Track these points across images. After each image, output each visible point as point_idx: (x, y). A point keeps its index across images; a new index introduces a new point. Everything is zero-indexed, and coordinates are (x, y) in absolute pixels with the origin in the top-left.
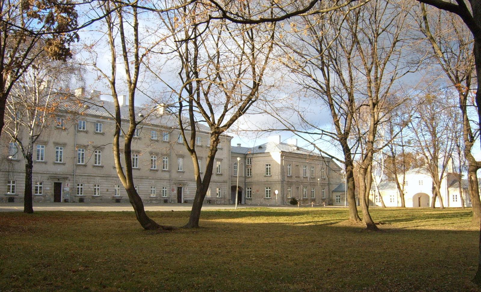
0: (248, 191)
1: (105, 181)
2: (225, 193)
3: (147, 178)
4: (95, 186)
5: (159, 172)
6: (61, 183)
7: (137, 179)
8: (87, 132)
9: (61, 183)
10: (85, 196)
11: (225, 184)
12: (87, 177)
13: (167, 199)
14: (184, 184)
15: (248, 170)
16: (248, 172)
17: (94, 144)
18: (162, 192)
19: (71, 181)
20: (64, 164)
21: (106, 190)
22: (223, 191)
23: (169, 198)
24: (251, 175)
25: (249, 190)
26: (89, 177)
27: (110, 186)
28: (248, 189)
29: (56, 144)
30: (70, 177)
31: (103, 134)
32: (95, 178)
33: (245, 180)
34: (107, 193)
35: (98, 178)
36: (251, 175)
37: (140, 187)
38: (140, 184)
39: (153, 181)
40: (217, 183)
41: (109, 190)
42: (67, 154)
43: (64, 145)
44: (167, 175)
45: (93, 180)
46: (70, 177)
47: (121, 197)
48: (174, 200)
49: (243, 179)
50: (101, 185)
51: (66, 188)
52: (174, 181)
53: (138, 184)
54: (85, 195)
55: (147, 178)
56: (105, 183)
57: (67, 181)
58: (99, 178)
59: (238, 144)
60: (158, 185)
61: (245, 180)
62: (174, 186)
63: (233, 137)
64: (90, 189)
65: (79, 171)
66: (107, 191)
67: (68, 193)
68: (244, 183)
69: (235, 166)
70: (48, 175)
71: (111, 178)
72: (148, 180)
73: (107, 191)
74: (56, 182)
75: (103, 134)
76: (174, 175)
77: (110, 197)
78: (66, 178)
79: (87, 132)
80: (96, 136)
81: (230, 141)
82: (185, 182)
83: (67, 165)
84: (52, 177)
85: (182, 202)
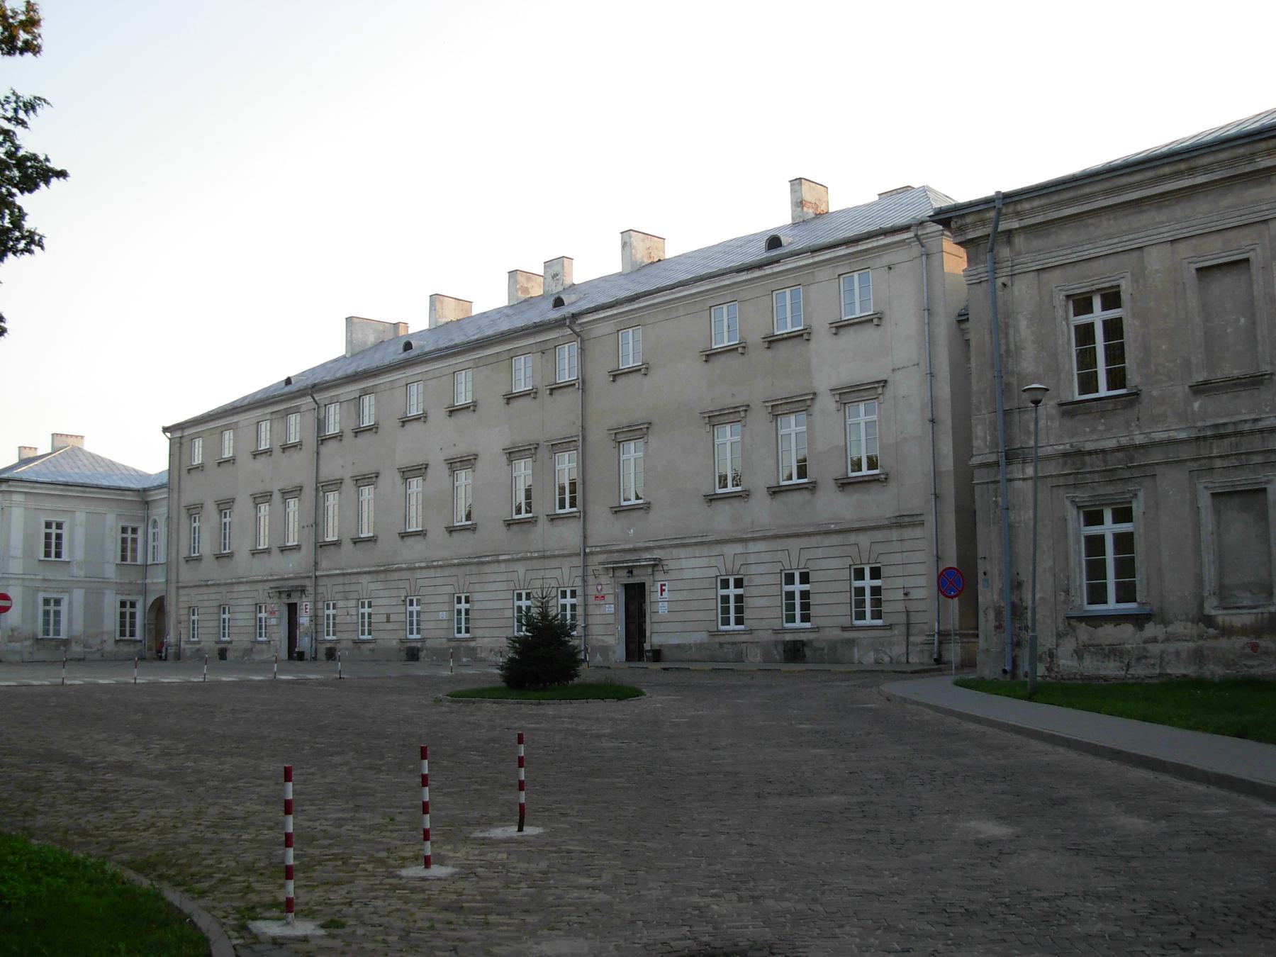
2: (915, 594)
5: (540, 525)
7: (467, 569)
11: (908, 533)
12: (340, 580)
34: (389, 626)
35: (365, 579)
38: (477, 587)
39: (521, 568)
40: (852, 538)
41: (392, 618)
44: (569, 535)
52: (602, 558)
54: (339, 636)
56: (382, 593)
62: (604, 579)
64: (348, 619)
71: (396, 576)
72: (503, 567)
76: (605, 529)
83: (304, 549)
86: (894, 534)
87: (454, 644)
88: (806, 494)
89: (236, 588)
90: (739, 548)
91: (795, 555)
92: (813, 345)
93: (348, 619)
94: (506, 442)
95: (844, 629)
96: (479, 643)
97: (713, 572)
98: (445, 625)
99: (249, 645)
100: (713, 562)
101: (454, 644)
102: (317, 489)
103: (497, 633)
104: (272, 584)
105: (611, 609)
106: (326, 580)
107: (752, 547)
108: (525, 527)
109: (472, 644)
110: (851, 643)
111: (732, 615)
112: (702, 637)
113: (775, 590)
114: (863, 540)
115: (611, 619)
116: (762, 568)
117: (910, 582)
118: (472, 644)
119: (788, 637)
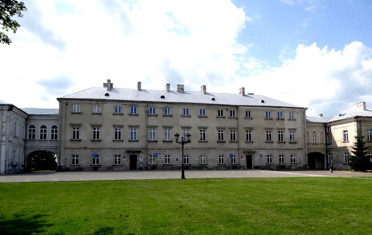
0: (330, 157)
1: (175, 152)
2: (301, 159)
3: (215, 148)
4: (220, 156)
6: (136, 156)
7: (205, 150)
8: (156, 116)
9: (136, 156)
10: (157, 165)
13: (236, 165)
14: (254, 153)
15: (329, 137)
16: (329, 139)
17: (163, 125)
18: (230, 159)
19: (144, 154)
20: (138, 141)
21: (176, 160)
22: (299, 158)
23: (237, 164)
24: (331, 142)
25: (331, 156)
26: (160, 150)
27: (179, 156)
28: (330, 155)
29: (131, 127)
30: (142, 150)
31: (171, 116)
32: (166, 150)
33: (327, 147)
35: (167, 151)
36: (331, 142)
37: (208, 156)
39: (221, 151)
40: (291, 151)
41: (178, 160)
42: (140, 133)
43: (137, 127)
44: (235, 146)
45: (164, 152)
46: (142, 150)
47: (190, 165)
48: (243, 167)
49: (325, 146)
50: (171, 156)
51: (141, 159)
52: (242, 150)
53: (207, 154)
55: (215, 148)
56: (175, 154)
57: (141, 154)
58: (169, 150)
59: (319, 115)
60: (226, 154)
61: (327, 147)
62: (243, 154)
63: (307, 108)
64: (161, 159)
65: (150, 146)
66: (177, 160)
67: (142, 163)
68: (325, 150)
69: (314, 134)
70: (124, 150)
72: (216, 150)
73: (177, 160)
74: (132, 154)
75: (171, 116)
77: (179, 165)
78: (139, 152)
79: (156, 116)
80: (165, 118)
81: (304, 113)
82: (255, 150)
83: (140, 142)
84: (128, 151)
85: (253, 168)
86: (298, 151)
87: (201, 165)
88: (284, 144)
89: (103, 150)
90: (271, 151)
91: (281, 153)
92: (285, 121)
93: (161, 159)
94: (217, 126)
95: (290, 164)
96: (209, 165)
97: (267, 154)
98: (198, 161)
99: (111, 166)
100: (267, 152)
101: (201, 165)
102: (147, 127)
103: (214, 163)
104: (126, 150)
105: (245, 159)
106: (151, 150)
107: (274, 151)
108: (222, 143)
109: (207, 165)
110: (291, 166)
111: (221, 160)
112: (265, 165)
113: (274, 158)
114: (293, 151)
115: (244, 161)
116: (276, 154)
117: (300, 158)
118: (207, 165)
119: (281, 165)
